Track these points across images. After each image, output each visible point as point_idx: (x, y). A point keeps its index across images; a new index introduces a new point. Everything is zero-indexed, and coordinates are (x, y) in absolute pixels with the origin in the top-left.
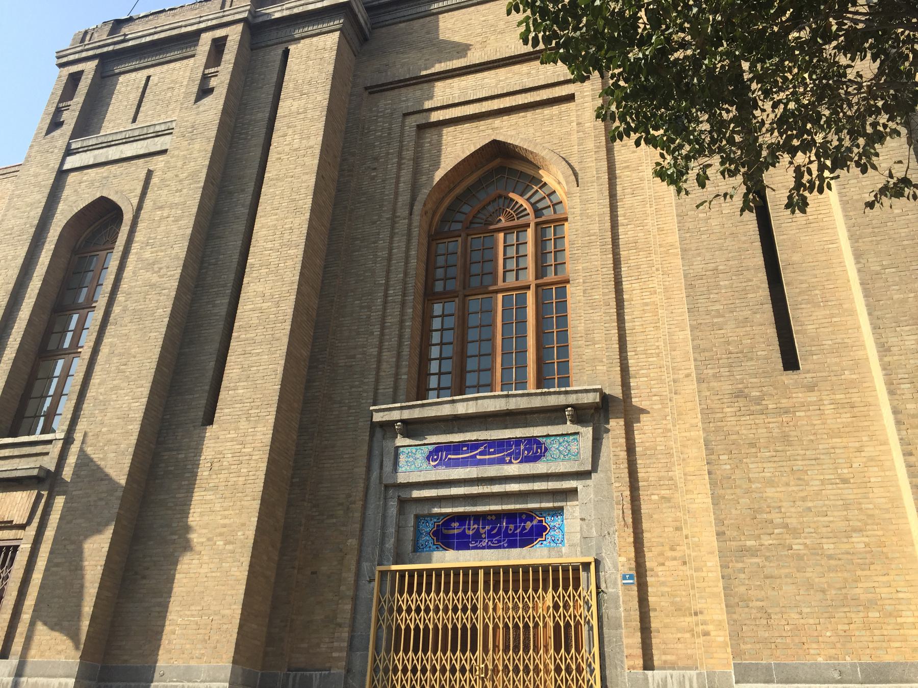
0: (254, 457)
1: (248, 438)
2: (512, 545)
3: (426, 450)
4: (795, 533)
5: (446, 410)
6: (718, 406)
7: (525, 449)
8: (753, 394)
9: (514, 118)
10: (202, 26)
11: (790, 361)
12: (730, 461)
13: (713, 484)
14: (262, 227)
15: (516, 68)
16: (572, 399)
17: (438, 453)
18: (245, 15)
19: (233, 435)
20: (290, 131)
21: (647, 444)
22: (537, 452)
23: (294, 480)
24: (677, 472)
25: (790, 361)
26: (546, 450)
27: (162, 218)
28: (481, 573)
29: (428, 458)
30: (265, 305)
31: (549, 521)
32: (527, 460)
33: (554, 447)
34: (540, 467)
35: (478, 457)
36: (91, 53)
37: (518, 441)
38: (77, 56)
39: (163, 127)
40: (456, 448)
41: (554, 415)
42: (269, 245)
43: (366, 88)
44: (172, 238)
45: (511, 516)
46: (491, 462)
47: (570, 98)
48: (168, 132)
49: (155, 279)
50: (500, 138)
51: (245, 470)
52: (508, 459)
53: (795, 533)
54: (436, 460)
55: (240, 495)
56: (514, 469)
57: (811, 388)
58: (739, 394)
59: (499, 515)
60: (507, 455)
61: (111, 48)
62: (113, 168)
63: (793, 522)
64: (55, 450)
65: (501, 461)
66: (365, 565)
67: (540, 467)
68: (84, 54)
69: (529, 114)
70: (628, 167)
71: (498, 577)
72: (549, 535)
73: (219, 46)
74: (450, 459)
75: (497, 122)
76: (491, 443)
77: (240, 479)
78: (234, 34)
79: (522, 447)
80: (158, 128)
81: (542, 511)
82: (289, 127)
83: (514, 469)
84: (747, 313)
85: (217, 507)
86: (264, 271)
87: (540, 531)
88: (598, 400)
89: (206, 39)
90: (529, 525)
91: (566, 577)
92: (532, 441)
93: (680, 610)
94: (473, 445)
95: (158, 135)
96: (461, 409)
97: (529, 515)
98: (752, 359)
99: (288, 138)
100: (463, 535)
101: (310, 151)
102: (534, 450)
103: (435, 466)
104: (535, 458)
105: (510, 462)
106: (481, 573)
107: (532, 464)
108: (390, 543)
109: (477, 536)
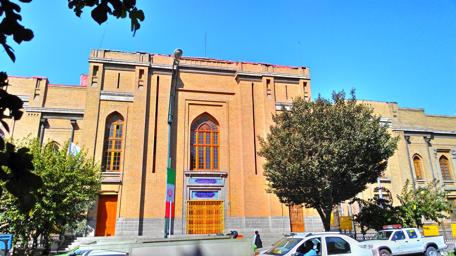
2: (209, 197)
4: (254, 199)
5: (199, 173)
11: (256, 174)
13: (245, 191)
15: (210, 94)
16: (222, 173)
17: (197, 181)
18: (149, 65)
20: (163, 102)
24: (237, 187)
25: (256, 174)
27: (136, 122)
31: (215, 193)
36: (100, 61)
37: (212, 179)
38: (96, 61)
39: (130, 94)
41: (219, 176)
45: (209, 192)
47: (221, 106)
48: (132, 96)
49: (137, 138)
53: (254, 199)
56: (211, 185)
57: (259, 178)
58: (249, 178)
61: (107, 62)
64: (121, 176)
65: (209, 183)
66: (184, 200)
68: (98, 61)
71: (209, 203)
72: (215, 195)
73: (142, 72)
78: (146, 70)
80: (128, 94)
83: (211, 185)
86: (161, 139)
87: (214, 195)
89: (138, 69)
90: (212, 194)
91: (218, 203)
93: (236, 208)
94: (204, 179)
95: (128, 96)
96: (202, 173)
97: (212, 192)
102: (215, 181)
104: (214, 183)
108: (188, 196)
109: (203, 195)
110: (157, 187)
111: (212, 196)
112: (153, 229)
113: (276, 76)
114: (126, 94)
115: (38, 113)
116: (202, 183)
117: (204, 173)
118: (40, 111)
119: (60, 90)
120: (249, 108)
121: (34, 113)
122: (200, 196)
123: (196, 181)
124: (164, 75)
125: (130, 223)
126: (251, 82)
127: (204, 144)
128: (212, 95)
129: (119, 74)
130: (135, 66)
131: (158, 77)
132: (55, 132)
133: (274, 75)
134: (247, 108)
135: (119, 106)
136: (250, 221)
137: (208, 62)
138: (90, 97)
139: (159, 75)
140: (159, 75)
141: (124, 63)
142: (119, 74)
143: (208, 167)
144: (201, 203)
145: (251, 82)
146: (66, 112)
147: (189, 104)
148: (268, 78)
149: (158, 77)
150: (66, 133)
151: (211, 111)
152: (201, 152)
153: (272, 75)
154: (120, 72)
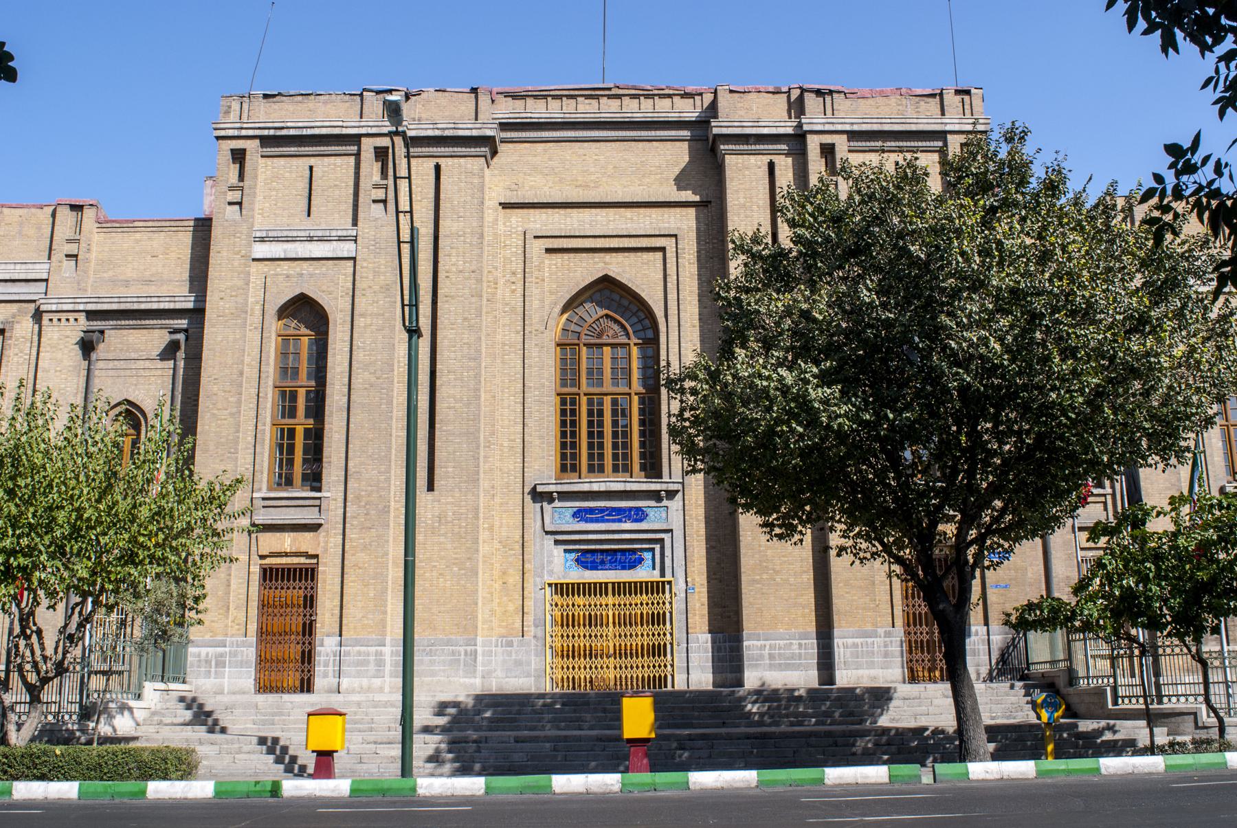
2: (624, 568)
3: (571, 511)
4: (777, 572)
10: (363, 131)
17: (579, 514)
19: (450, 499)
28: (610, 586)
32: (636, 521)
33: (651, 513)
34: (643, 526)
36: (251, 133)
37: (630, 509)
38: (236, 133)
40: (591, 510)
44: (380, 346)
46: (614, 521)
49: (373, 379)
50: (611, 274)
53: (777, 572)
59: (615, 551)
61: (272, 132)
62: (305, 264)
63: (778, 568)
65: (620, 521)
67: (643, 526)
68: (244, 133)
75: (608, 257)
76: (614, 509)
80: (340, 233)
81: (642, 550)
83: (628, 526)
85: (449, 546)
86: (452, 377)
87: (641, 560)
90: (633, 557)
92: (638, 509)
94: (602, 510)
96: (595, 487)
97: (634, 551)
100: (593, 562)
102: (640, 515)
104: (641, 520)
106: (610, 586)
109: (603, 562)
110: (442, 539)
111: (632, 565)
112: (433, 674)
113: (856, 128)
114: (334, 233)
115: (76, 315)
116: (597, 521)
117: (603, 487)
118: (81, 307)
119: (138, 236)
121: (63, 316)
122: (594, 567)
123: (574, 515)
124: (456, 160)
125: (359, 653)
126: (767, 159)
127: (608, 387)
128: (628, 213)
129: (311, 168)
130: (360, 136)
131: (438, 168)
132: (128, 373)
133: (848, 128)
135: (311, 275)
136: (763, 647)
137: (609, 97)
138: (224, 254)
139: (442, 161)
140: (442, 161)
141: (324, 131)
142: (311, 168)
143: (622, 466)
144: (599, 589)
145: (767, 159)
146: (155, 306)
147: (548, 251)
148: (828, 139)
149: (438, 168)
150: (159, 372)
151: (626, 270)
152: (595, 415)
153: (839, 127)
154: (312, 161)
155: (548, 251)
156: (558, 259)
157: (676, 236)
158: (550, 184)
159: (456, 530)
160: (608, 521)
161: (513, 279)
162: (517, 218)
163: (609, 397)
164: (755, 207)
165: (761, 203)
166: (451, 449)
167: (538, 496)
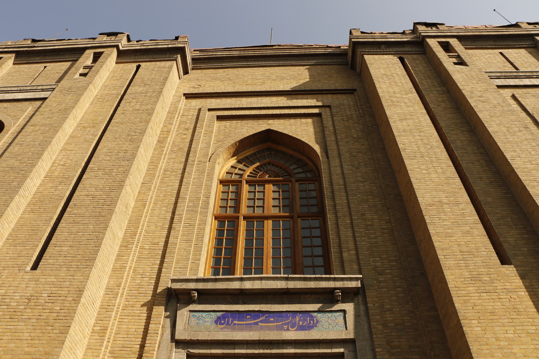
0: (68, 299)
1: (66, 283)
6: (462, 286)
7: (300, 320)
8: (485, 279)
9: (282, 121)
12: (480, 325)
14: (105, 147)
17: (223, 319)
19: (52, 279)
20: (134, 101)
21: (397, 321)
22: (310, 323)
23: (96, 328)
26: (318, 322)
29: (216, 322)
30: (97, 193)
32: (302, 328)
35: (260, 324)
42: (108, 158)
43: (184, 94)
44: (37, 143)
49: (17, 164)
51: (58, 308)
52: (286, 327)
54: (223, 324)
55: (50, 328)
60: (285, 324)
67: (314, 335)
69: (292, 121)
70: (360, 152)
74: (235, 324)
77: (52, 314)
79: (297, 319)
82: (133, 99)
84: (467, 228)
86: (100, 173)
88: (359, 286)
95: (43, 90)
96: (248, 285)
98: (478, 257)
99: (132, 104)
101: (146, 111)
103: (222, 329)
104: (309, 328)
105: (288, 330)
107: (306, 332)
117: (257, 285)
120: (407, 94)
123: (218, 321)
134: (398, 95)
140: (140, 64)
147: (219, 118)
155: (219, 118)
156: (227, 123)
157: (329, 107)
158: (226, 84)
159: (44, 316)
160: (262, 328)
161: (186, 132)
162: (196, 103)
163: (270, 222)
164: (395, 75)
165: (399, 73)
166: (74, 230)
167: (174, 299)
